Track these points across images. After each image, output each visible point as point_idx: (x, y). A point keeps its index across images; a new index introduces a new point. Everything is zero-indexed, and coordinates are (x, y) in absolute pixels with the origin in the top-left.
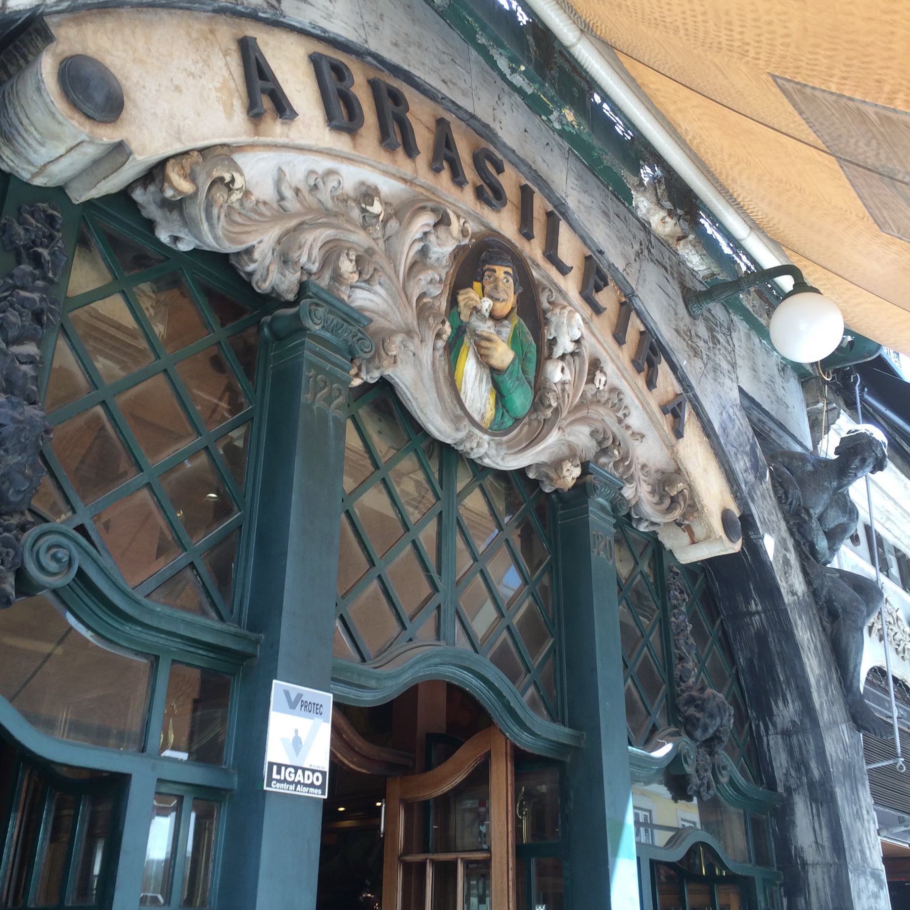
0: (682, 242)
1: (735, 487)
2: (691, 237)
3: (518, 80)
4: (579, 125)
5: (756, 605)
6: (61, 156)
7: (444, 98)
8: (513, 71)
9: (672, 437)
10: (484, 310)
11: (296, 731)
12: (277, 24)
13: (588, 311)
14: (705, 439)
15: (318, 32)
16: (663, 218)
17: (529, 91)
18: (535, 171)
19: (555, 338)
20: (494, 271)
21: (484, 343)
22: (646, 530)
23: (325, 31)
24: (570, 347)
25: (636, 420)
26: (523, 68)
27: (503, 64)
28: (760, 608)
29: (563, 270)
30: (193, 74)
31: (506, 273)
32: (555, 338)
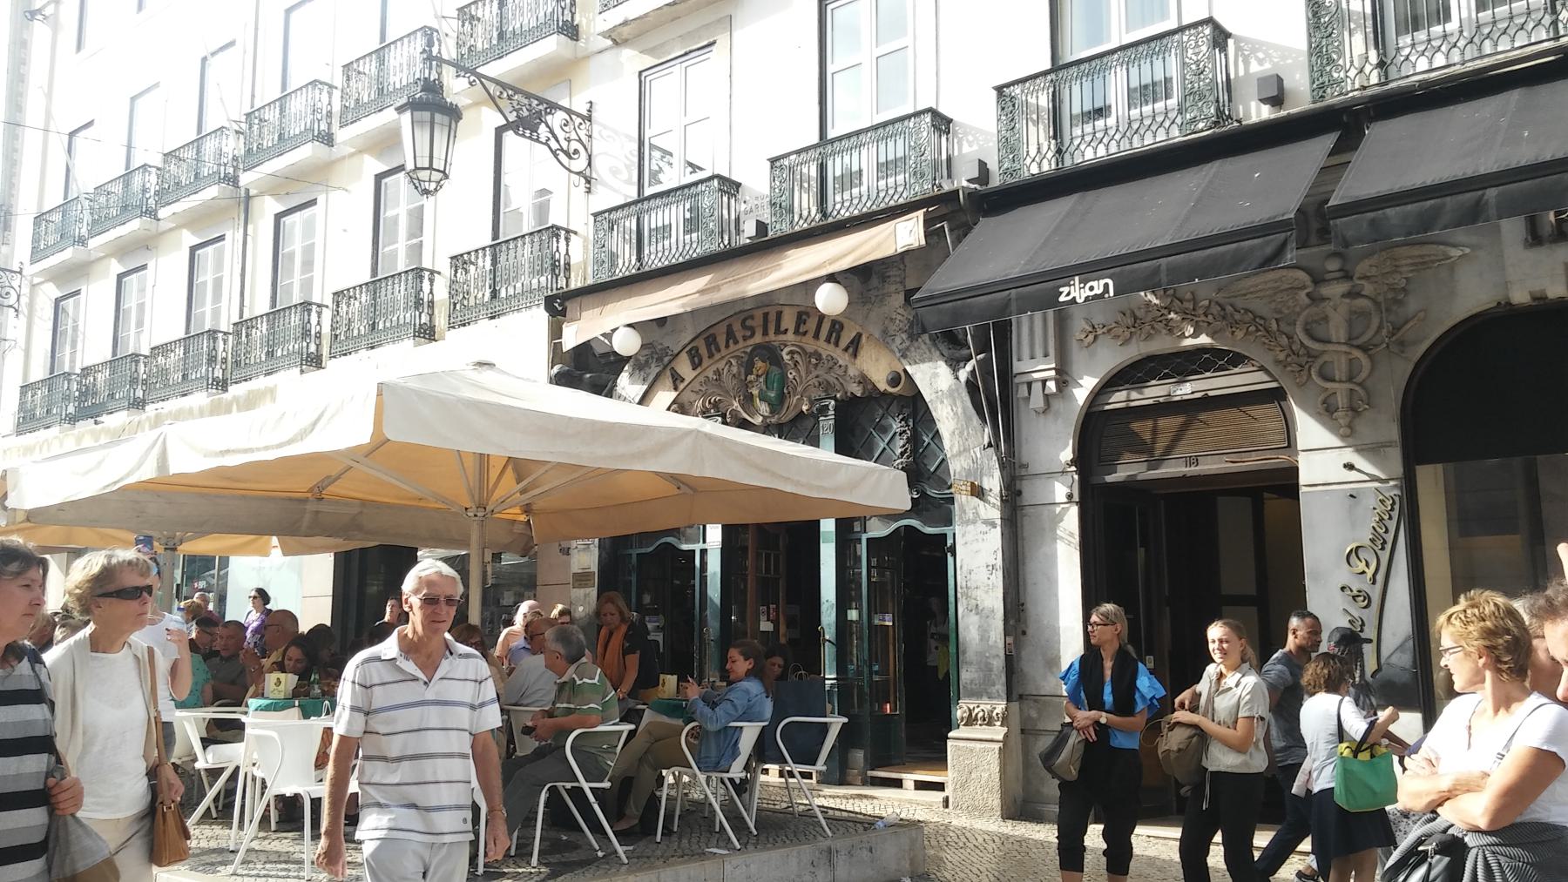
13: (799, 338)
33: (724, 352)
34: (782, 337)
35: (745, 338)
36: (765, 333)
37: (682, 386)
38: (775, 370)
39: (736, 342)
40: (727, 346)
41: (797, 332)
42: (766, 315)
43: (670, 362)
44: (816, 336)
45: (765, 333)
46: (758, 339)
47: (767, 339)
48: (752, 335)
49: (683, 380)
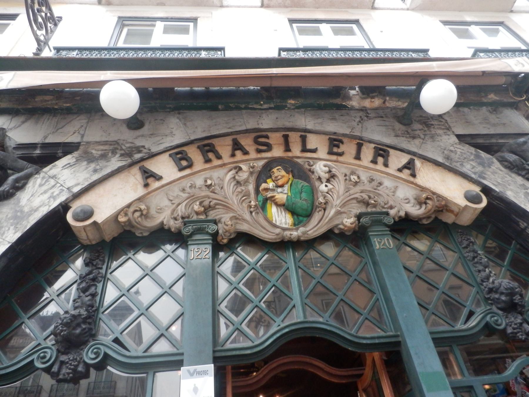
0: (387, 103)
1: (469, 179)
2: (388, 98)
3: (265, 106)
4: (298, 101)
5: (523, 224)
6: (87, 234)
7: (232, 132)
8: (261, 105)
9: (411, 179)
10: (271, 188)
11: (195, 385)
12: (152, 156)
13: (334, 158)
14: (440, 167)
15: (170, 148)
16: (371, 101)
17: (272, 105)
18: (285, 128)
19: (319, 176)
20: (273, 171)
21: (273, 199)
22: (428, 222)
23: (171, 146)
24: (327, 176)
25: (388, 183)
26: (262, 103)
27: (255, 106)
28: (525, 224)
29: (314, 151)
30: (121, 188)
31: (278, 169)
32: (319, 176)
33: (226, 158)
34: (309, 155)
35: (259, 151)
36: (288, 149)
37: (156, 184)
38: (301, 183)
39: (246, 153)
40: (233, 155)
41: (331, 153)
42: (286, 138)
43: (142, 160)
44: (358, 157)
45: (288, 149)
46: (277, 152)
47: (290, 154)
48: (269, 148)
49: (159, 178)
